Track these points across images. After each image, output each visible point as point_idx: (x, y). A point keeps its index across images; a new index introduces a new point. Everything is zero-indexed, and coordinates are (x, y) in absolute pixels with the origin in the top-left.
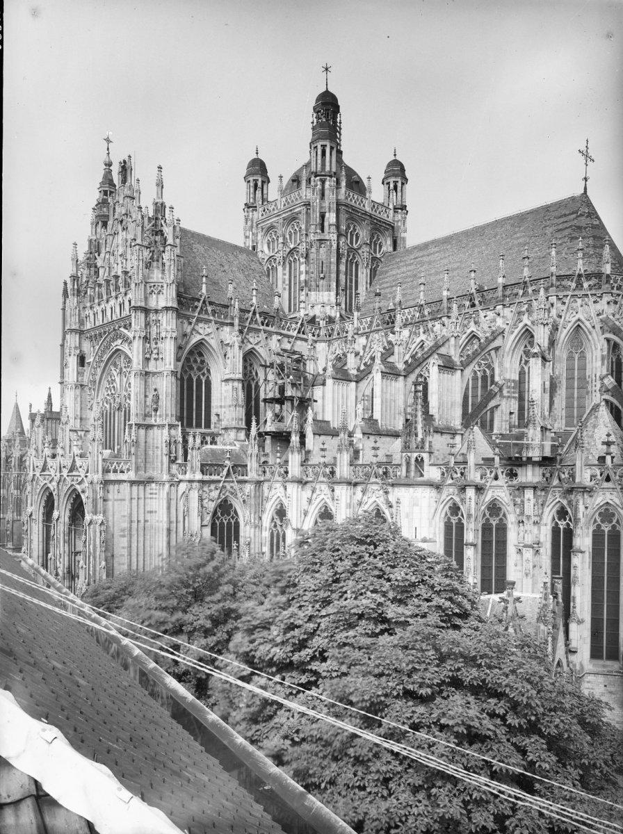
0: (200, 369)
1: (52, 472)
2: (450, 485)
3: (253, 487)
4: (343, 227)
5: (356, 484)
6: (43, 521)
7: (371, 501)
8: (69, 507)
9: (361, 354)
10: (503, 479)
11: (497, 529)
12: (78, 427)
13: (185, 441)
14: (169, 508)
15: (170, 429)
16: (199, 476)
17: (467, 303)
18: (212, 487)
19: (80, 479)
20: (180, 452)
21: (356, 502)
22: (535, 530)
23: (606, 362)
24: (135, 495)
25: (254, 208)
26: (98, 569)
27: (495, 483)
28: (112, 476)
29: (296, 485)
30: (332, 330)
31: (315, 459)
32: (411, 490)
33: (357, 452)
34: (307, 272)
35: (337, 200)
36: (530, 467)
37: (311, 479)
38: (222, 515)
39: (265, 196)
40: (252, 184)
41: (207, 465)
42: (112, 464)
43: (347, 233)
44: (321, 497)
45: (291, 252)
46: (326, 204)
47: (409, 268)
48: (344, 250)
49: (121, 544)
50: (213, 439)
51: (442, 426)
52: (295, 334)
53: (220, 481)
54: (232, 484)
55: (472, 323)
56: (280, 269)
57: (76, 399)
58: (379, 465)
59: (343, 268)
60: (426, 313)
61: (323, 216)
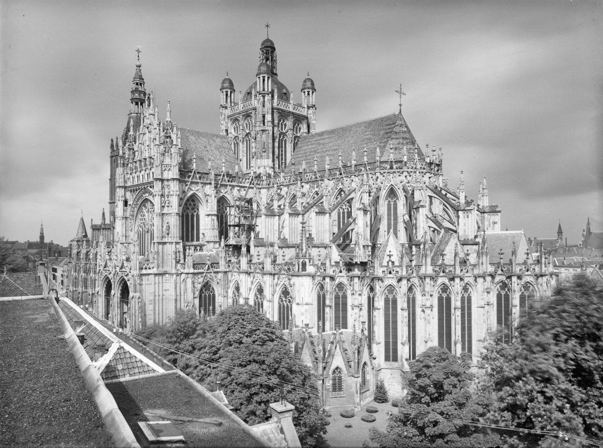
0: (193, 209)
1: (110, 269)
2: (319, 276)
3: (222, 275)
4: (276, 122)
5: (274, 275)
6: (105, 296)
7: (282, 283)
8: (120, 288)
9: (285, 197)
10: (344, 272)
11: (342, 298)
12: (124, 241)
13: (185, 250)
14: (176, 288)
15: (176, 245)
16: (192, 271)
17: (338, 173)
18: (200, 276)
19: (126, 273)
20: (182, 256)
21: (275, 284)
22: (360, 298)
23: (405, 207)
24: (157, 281)
25: (226, 108)
26: (137, 322)
27: (340, 274)
28: (144, 272)
29: (244, 274)
30: (270, 182)
31: (255, 260)
32: (300, 278)
33: (275, 257)
34: (255, 147)
35: (272, 106)
36: (356, 266)
37: (252, 271)
38: (205, 291)
39: (232, 100)
40: (225, 93)
41: (196, 264)
42: (144, 265)
43: (279, 124)
44: (258, 280)
45: (247, 134)
46: (265, 109)
47: (313, 146)
48: (277, 134)
49: (149, 308)
50: (201, 247)
51: (318, 244)
52: (248, 185)
53: (204, 273)
55: (340, 184)
56: (241, 144)
57: (123, 225)
58: (286, 264)
59: (276, 144)
60: (318, 177)
61: (264, 117)
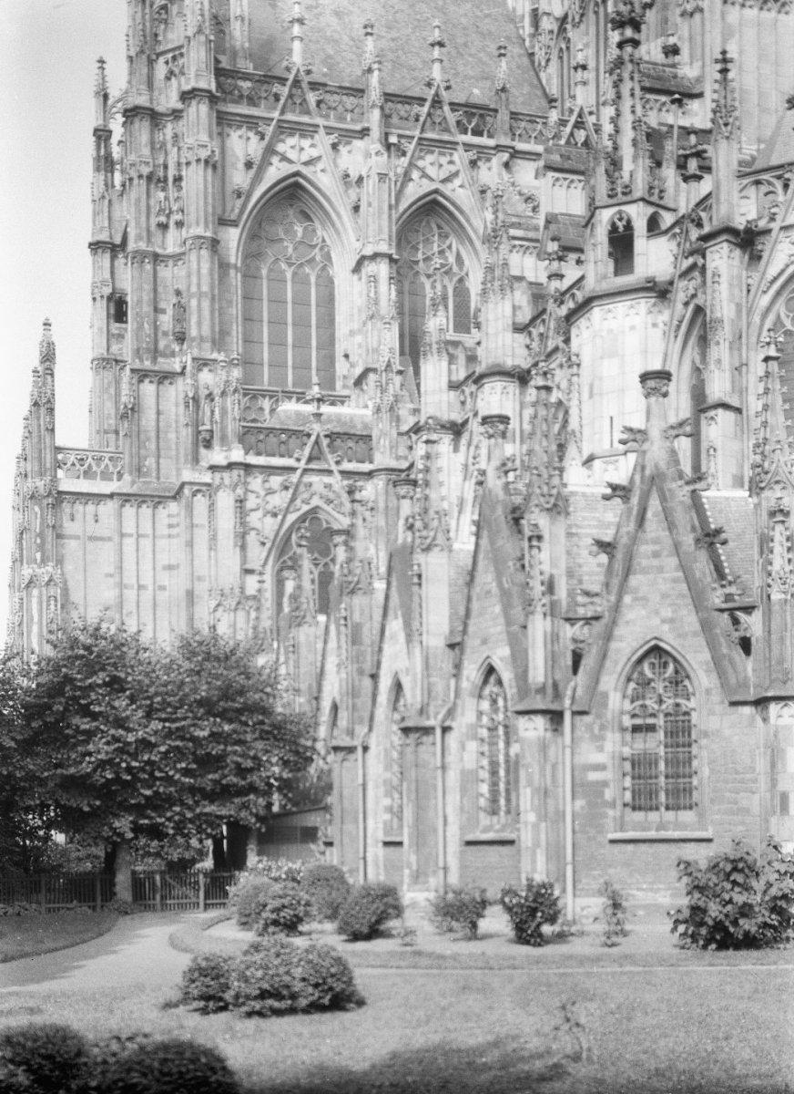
18: (276, 481)
24: (129, 527)
54: (327, 479)
